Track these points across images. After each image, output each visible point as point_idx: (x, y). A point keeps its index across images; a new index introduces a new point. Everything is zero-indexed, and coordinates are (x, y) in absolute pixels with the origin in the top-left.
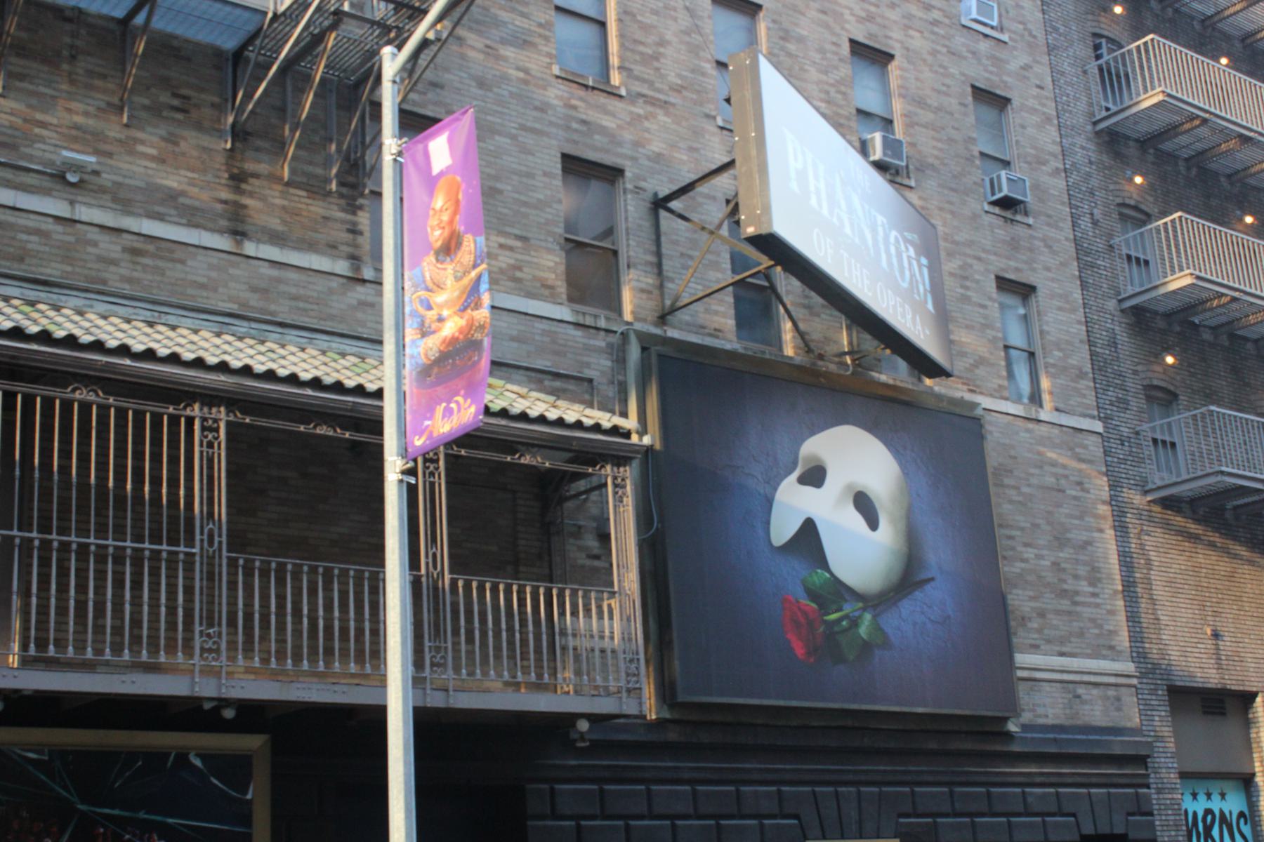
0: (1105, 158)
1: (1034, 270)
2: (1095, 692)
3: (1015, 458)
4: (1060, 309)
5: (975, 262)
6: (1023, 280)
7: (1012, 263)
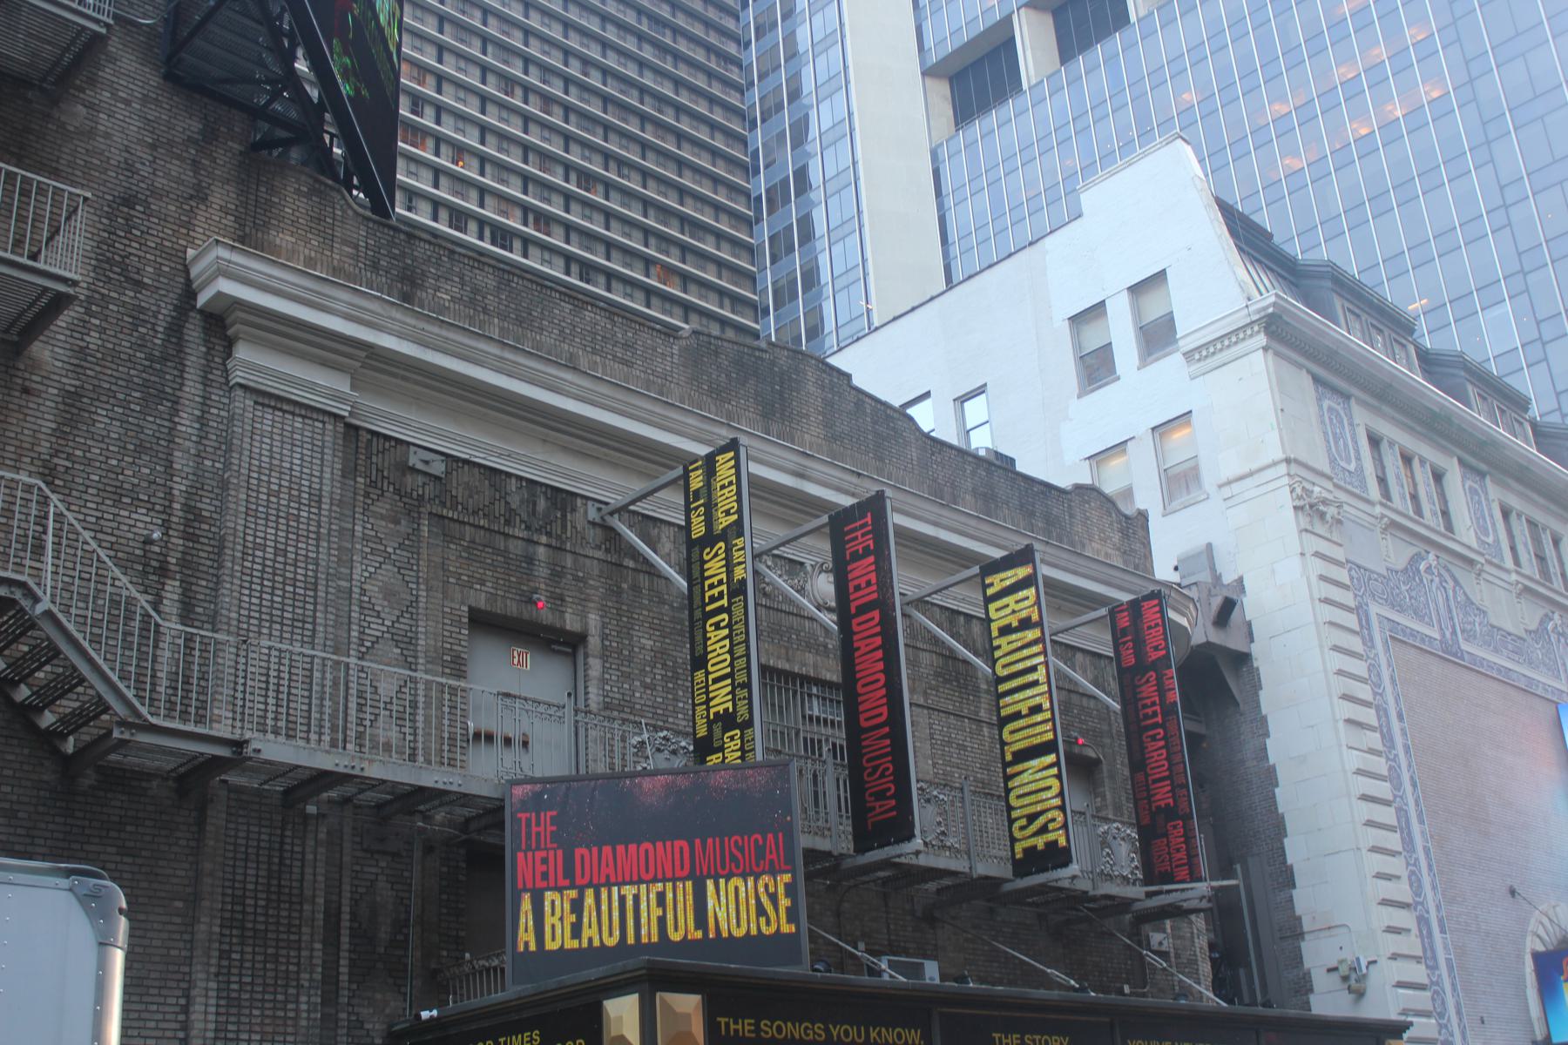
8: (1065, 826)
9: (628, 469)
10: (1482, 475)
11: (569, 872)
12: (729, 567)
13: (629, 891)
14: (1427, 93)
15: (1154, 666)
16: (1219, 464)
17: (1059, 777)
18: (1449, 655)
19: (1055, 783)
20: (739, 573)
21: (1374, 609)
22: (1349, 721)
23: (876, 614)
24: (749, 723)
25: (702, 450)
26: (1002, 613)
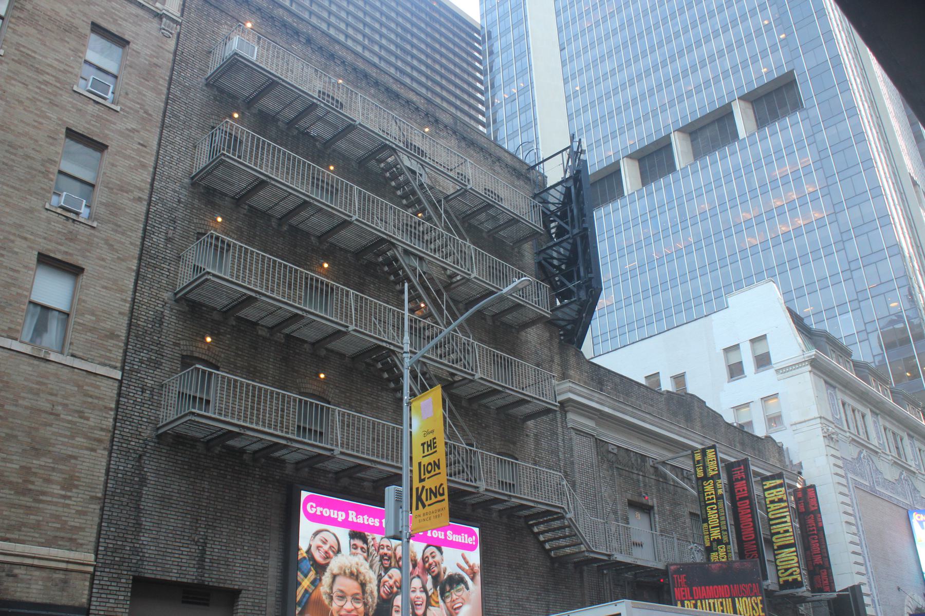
0: (196, 202)
1: (85, 257)
2: (37, 573)
3: (7, 382)
4: (105, 288)
5: (18, 239)
6: (72, 262)
7: (63, 248)
8: (800, 573)
9: (669, 450)
10: (877, 415)
11: (692, 595)
12: (716, 489)
13: (711, 601)
14: (814, 215)
15: (812, 512)
16: (790, 416)
17: (797, 556)
18: (873, 493)
19: (796, 558)
20: (720, 492)
21: (849, 475)
22: (847, 522)
23: (747, 501)
24: (729, 544)
25: (700, 447)
26: (771, 495)
